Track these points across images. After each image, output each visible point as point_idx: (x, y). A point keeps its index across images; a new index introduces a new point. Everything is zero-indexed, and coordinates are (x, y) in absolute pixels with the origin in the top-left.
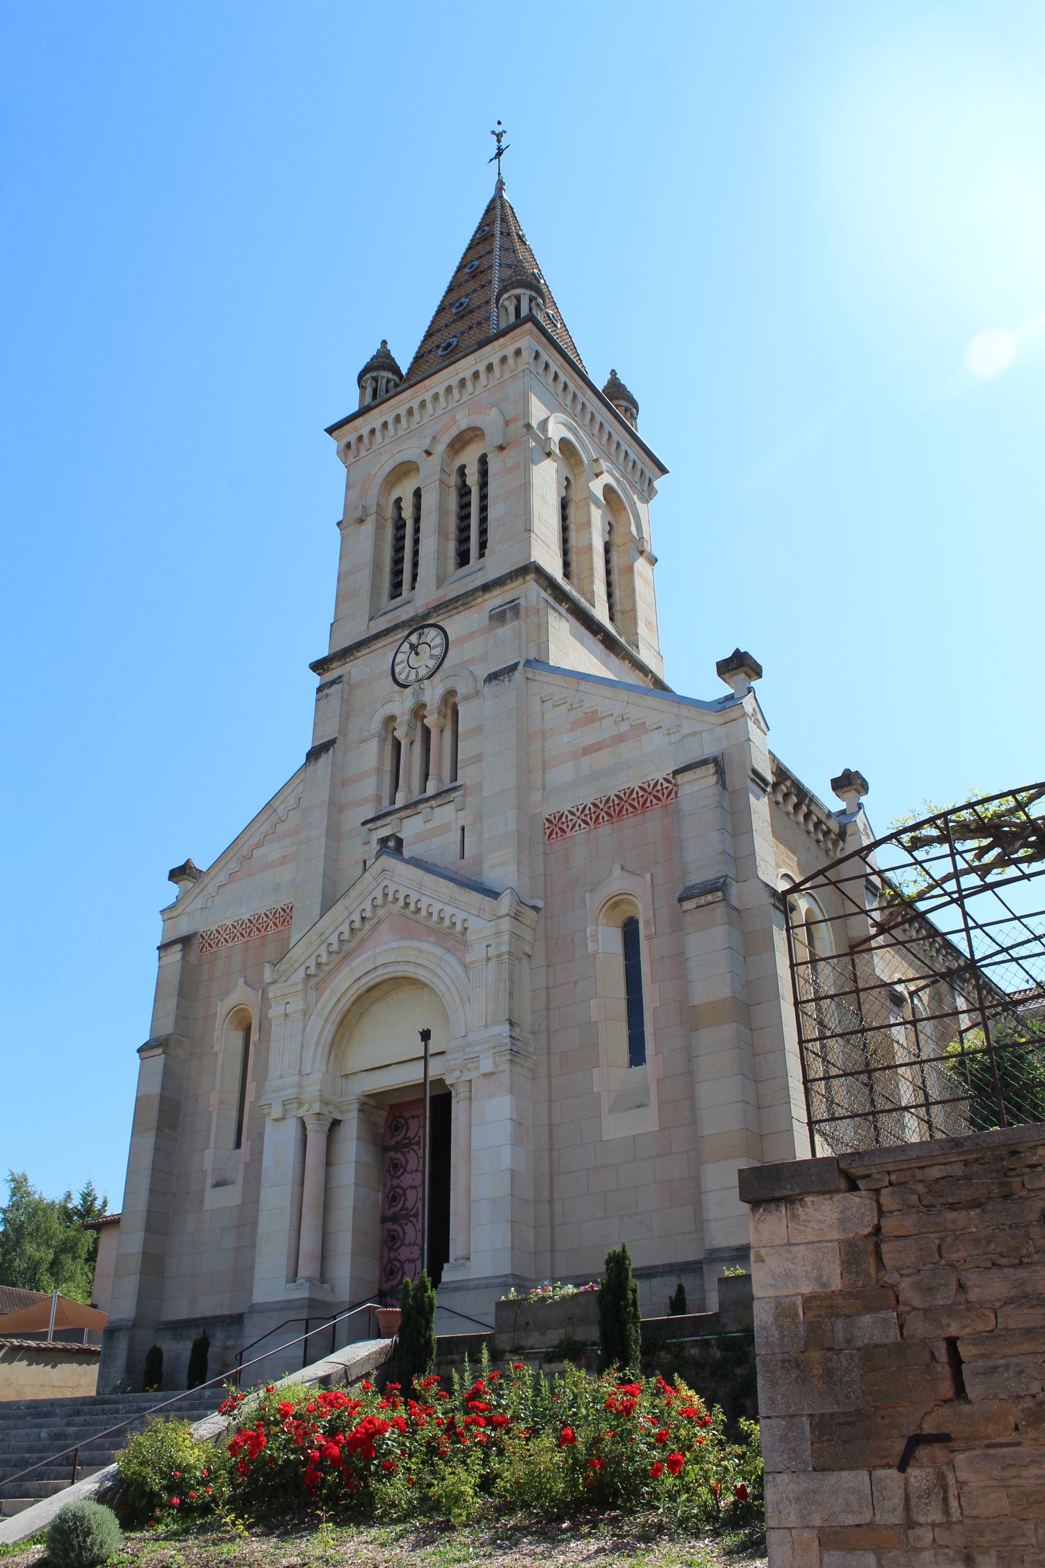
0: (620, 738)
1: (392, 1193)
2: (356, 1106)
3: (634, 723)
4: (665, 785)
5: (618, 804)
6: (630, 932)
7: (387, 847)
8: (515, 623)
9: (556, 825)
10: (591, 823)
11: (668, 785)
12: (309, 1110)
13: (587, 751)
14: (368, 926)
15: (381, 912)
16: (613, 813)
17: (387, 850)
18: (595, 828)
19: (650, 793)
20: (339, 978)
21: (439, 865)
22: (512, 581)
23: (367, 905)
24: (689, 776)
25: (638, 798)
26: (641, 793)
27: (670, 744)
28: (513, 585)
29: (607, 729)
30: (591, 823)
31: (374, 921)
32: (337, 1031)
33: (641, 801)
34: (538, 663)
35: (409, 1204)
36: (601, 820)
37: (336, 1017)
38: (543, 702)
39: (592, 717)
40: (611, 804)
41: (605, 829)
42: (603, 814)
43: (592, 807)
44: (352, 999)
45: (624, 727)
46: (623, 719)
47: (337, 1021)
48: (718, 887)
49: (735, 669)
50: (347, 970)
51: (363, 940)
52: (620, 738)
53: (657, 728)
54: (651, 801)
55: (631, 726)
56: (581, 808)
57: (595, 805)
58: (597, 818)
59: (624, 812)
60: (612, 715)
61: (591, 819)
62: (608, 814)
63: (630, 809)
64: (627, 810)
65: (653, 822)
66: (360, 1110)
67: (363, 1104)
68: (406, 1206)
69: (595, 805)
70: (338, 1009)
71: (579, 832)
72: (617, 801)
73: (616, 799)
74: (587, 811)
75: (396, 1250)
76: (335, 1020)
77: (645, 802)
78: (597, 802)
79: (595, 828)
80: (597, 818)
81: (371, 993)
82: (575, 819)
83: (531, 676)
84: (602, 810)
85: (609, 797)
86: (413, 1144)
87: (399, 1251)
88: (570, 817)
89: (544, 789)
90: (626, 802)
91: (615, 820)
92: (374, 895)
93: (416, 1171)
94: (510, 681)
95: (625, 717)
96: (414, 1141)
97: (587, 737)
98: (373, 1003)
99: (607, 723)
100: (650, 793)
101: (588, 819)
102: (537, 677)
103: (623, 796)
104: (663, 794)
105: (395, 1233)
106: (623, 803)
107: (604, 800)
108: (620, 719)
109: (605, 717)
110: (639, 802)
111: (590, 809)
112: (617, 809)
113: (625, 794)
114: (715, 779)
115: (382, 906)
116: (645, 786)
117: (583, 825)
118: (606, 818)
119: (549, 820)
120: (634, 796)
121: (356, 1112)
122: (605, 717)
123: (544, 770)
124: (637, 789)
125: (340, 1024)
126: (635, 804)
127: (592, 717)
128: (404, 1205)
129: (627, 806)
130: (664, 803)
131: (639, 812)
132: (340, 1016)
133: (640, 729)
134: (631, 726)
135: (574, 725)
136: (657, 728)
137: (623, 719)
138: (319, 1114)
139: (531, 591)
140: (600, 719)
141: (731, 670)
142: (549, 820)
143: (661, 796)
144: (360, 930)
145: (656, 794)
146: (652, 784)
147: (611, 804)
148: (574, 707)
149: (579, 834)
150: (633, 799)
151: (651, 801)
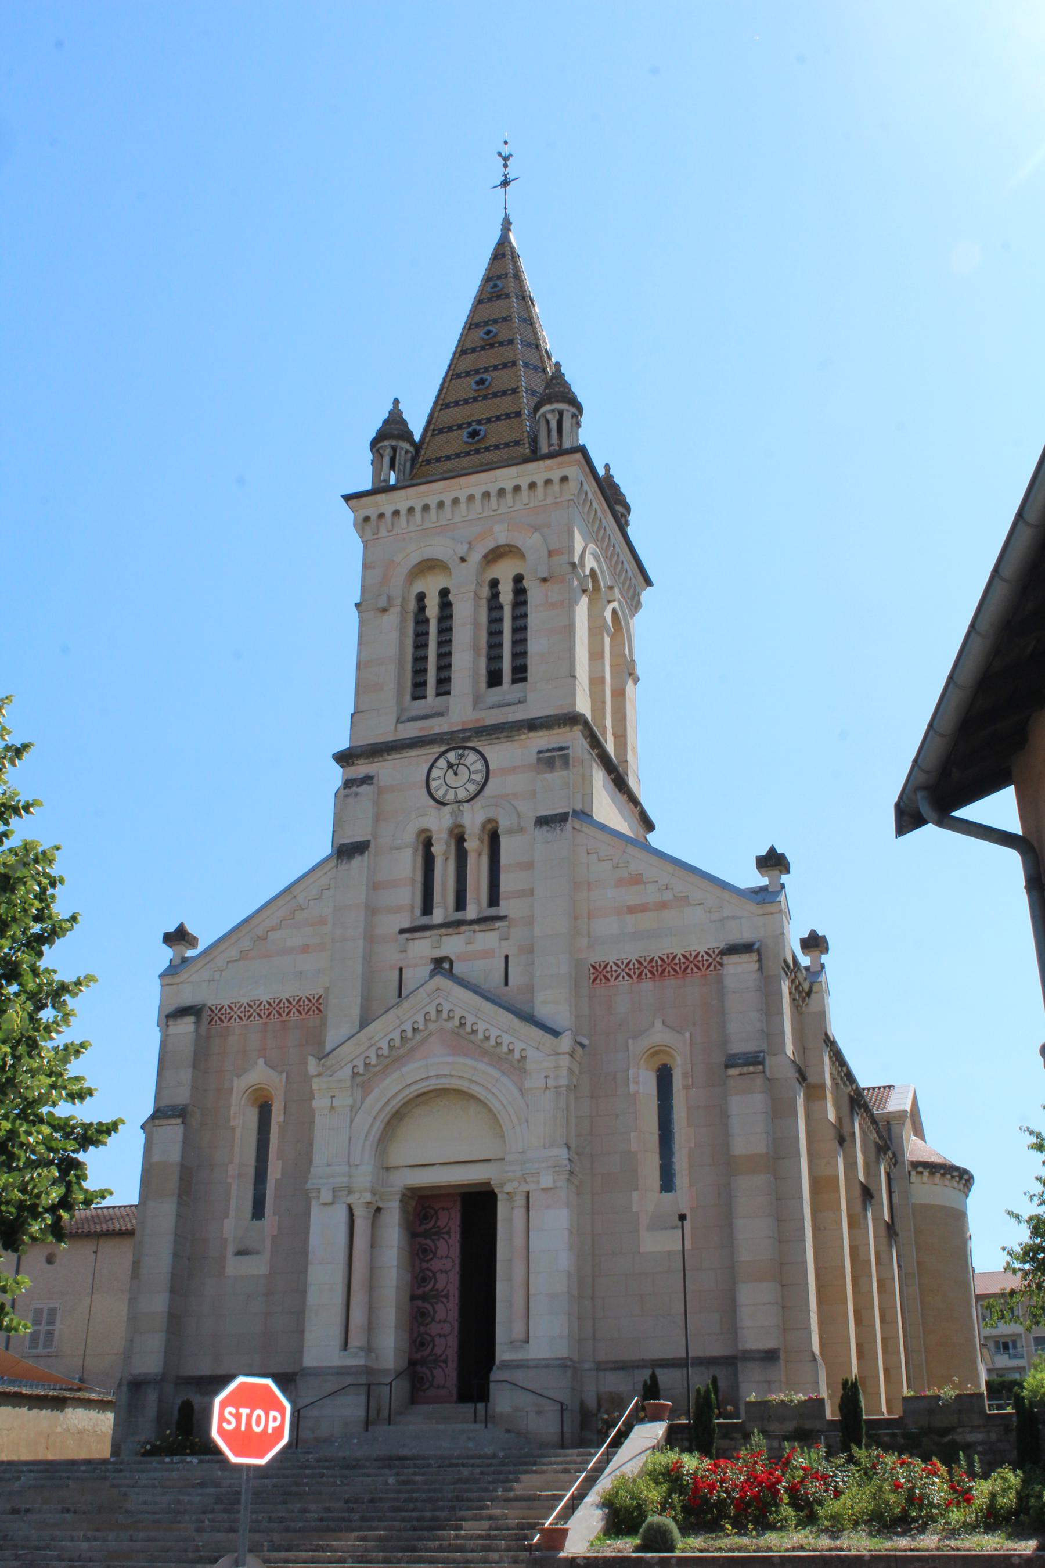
0: (663, 906)
1: (421, 1275)
2: (398, 1197)
3: (679, 895)
4: (706, 957)
5: (661, 966)
6: (664, 1078)
7: (444, 969)
8: (565, 773)
9: (600, 973)
10: (635, 977)
11: (709, 958)
12: (360, 1200)
13: (631, 910)
14: (418, 1037)
15: (432, 1027)
16: (656, 973)
17: (443, 971)
18: (638, 982)
19: (691, 962)
20: (388, 1080)
21: (483, 987)
22: (559, 728)
23: (420, 1018)
24: (734, 959)
25: (680, 963)
26: (683, 960)
27: (711, 922)
28: (560, 731)
29: (651, 895)
30: (635, 977)
31: (426, 1033)
32: (385, 1128)
33: (683, 966)
34: (584, 815)
35: (440, 1285)
36: (644, 976)
37: (385, 1115)
38: (588, 853)
39: (637, 880)
40: (654, 964)
41: (647, 985)
42: (646, 971)
43: (636, 963)
44: (402, 1102)
45: (668, 896)
46: (667, 889)
47: (386, 1120)
48: (755, 1060)
49: (772, 866)
50: (397, 1074)
51: (413, 1049)
52: (663, 906)
53: (699, 904)
54: (692, 969)
55: (675, 896)
56: (625, 962)
57: (639, 962)
58: (640, 974)
59: (666, 974)
60: (657, 882)
61: (634, 973)
62: (651, 972)
63: (672, 972)
64: (669, 972)
65: (693, 989)
66: (401, 1201)
67: (404, 1195)
68: (436, 1287)
69: (639, 962)
70: (388, 1108)
71: (622, 983)
72: (660, 963)
73: (659, 961)
74: (631, 966)
75: (426, 1325)
76: (384, 1118)
77: (686, 968)
78: (642, 960)
79: (638, 982)
80: (640, 974)
81: (419, 1099)
82: (619, 971)
83: (577, 826)
84: (646, 967)
85: (653, 958)
86: (444, 1233)
87: (429, 1326)
88: (615, 968)
89: (589, 937)
90: (668, 965)
91: (657, 978)
92: (427, 1009)
93: (446, 1257)
94: (562, 830)
95: (669, 887)
96: (444, 1230)
97: (632, 896)
98: (416, 1106)
99: (651, 888)
100: (691, 962)
101: (631, 973)
102: (584, 829)
103: (666, 960)
104: (703, 965)
105: (425, 1310)
106: (665, 966)
107: (648, 959)
108: (664, 887)
109: (649, 882)
110: (680, 968)
111: (634, 964)
112: (660, 969)
113: (668, 958)
114: (757, 966)
115: (435, 1021)
116: (688, 955)
117: (627, 978)
118: (649, 975)
119: (593, 967)
120: (677, 961)
121: (398, 1202)
122: (649, 882)
123: (589, 919)
124: (679, 956)
125: (388, 1123)
126: (677, 968)
127: (637, 880)
128: (434, 1285)
129: (669, 968)
130: (703, 973)
131: (680, 976)
132: (389, 1116)
133: (683, 900)
134: (675, 896)
135: (620, 883)
136: (699, 904)
137: (667, 889)
138: (369, 1203)
139: (575, 739)
140: (644, 883)
141: (768, 867)
142: (593, 967)
143: (701, 967)
144: (411, 1039)
145: (697, 963)
146: (694, 954)
147: (654, 964)
148: (619, 866)
149: (623, 984)
150: (676, 964)
151: (692, 969)
